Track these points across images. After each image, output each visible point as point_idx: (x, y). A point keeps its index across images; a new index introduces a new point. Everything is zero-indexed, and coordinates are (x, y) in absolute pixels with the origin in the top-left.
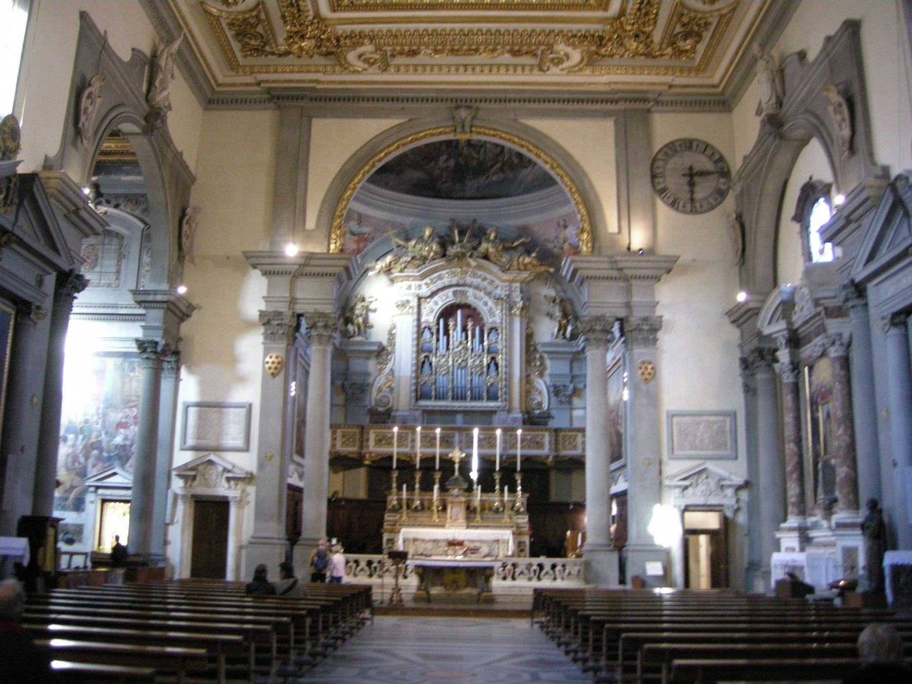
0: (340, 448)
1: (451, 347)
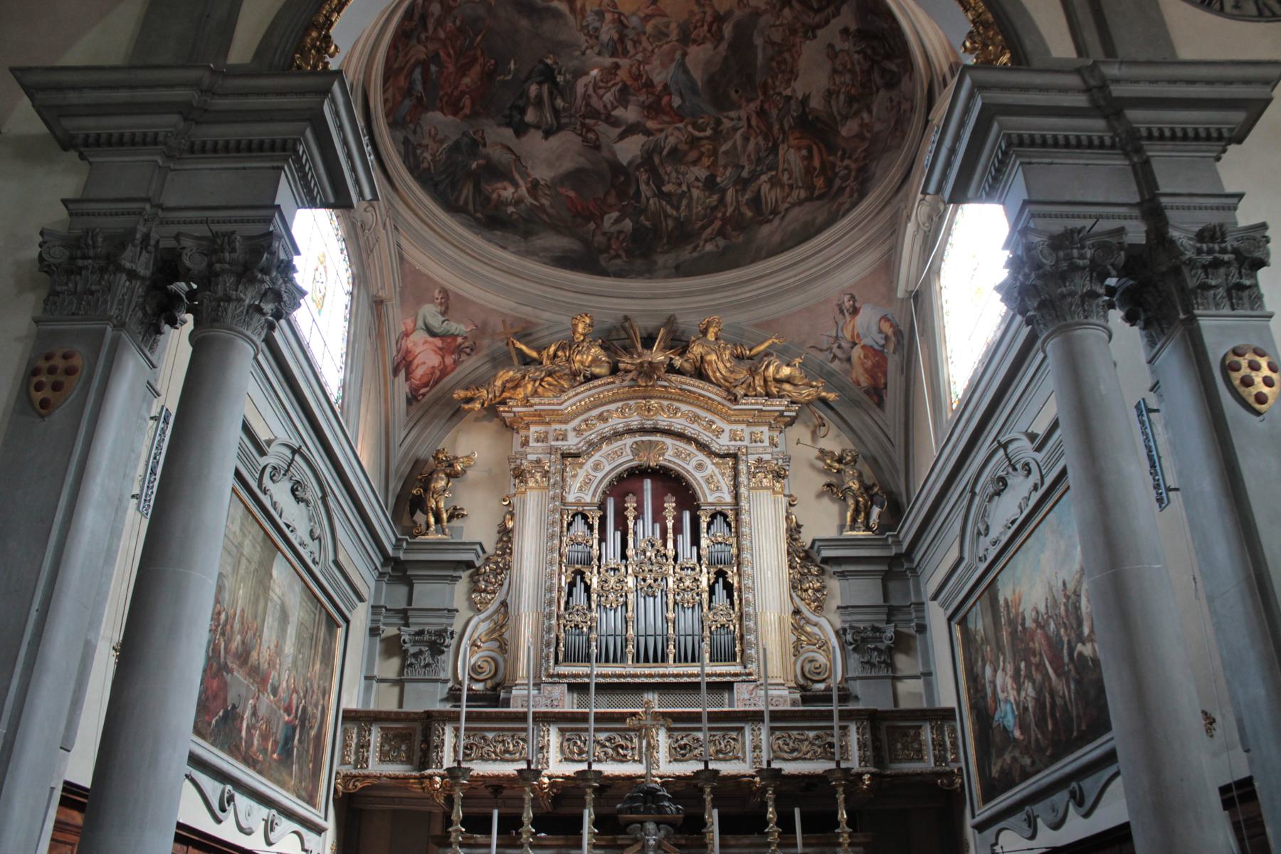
0: (375, 767)
1: (630, 552)
